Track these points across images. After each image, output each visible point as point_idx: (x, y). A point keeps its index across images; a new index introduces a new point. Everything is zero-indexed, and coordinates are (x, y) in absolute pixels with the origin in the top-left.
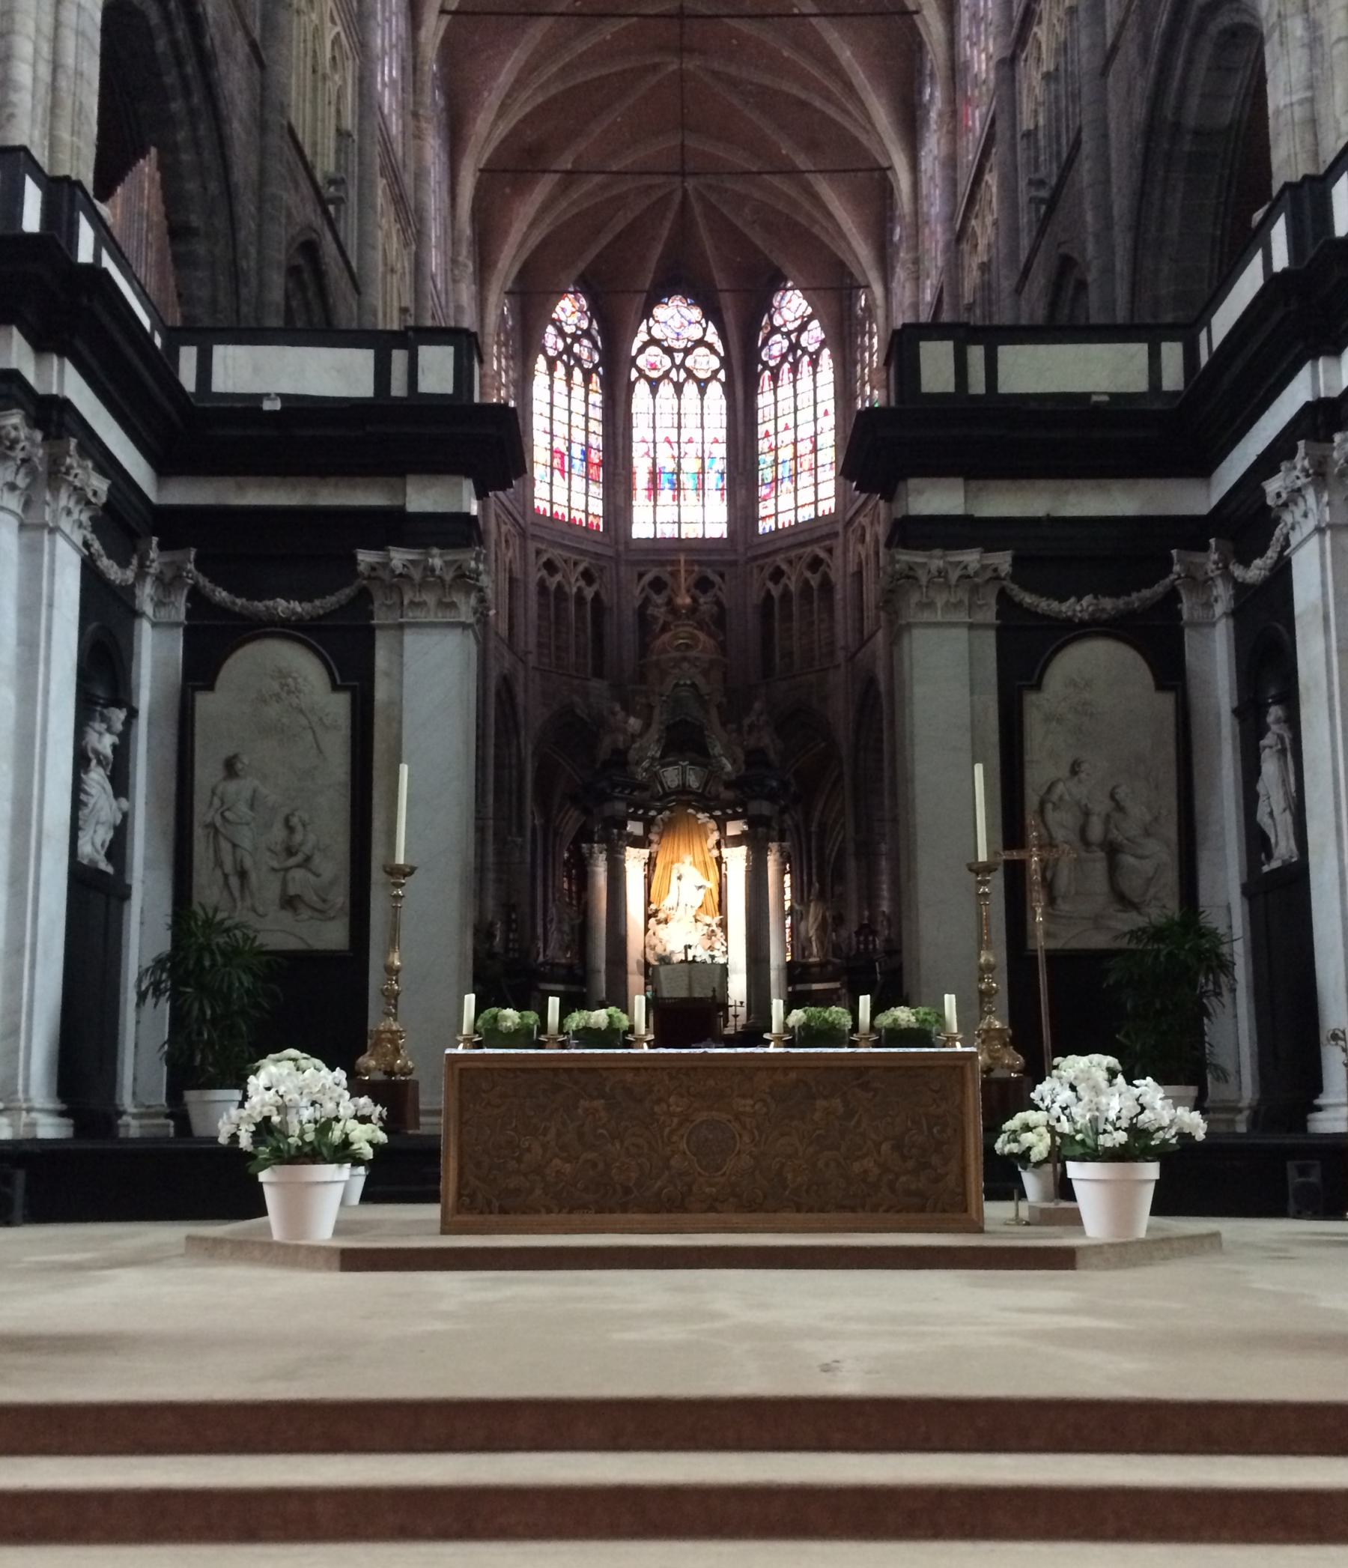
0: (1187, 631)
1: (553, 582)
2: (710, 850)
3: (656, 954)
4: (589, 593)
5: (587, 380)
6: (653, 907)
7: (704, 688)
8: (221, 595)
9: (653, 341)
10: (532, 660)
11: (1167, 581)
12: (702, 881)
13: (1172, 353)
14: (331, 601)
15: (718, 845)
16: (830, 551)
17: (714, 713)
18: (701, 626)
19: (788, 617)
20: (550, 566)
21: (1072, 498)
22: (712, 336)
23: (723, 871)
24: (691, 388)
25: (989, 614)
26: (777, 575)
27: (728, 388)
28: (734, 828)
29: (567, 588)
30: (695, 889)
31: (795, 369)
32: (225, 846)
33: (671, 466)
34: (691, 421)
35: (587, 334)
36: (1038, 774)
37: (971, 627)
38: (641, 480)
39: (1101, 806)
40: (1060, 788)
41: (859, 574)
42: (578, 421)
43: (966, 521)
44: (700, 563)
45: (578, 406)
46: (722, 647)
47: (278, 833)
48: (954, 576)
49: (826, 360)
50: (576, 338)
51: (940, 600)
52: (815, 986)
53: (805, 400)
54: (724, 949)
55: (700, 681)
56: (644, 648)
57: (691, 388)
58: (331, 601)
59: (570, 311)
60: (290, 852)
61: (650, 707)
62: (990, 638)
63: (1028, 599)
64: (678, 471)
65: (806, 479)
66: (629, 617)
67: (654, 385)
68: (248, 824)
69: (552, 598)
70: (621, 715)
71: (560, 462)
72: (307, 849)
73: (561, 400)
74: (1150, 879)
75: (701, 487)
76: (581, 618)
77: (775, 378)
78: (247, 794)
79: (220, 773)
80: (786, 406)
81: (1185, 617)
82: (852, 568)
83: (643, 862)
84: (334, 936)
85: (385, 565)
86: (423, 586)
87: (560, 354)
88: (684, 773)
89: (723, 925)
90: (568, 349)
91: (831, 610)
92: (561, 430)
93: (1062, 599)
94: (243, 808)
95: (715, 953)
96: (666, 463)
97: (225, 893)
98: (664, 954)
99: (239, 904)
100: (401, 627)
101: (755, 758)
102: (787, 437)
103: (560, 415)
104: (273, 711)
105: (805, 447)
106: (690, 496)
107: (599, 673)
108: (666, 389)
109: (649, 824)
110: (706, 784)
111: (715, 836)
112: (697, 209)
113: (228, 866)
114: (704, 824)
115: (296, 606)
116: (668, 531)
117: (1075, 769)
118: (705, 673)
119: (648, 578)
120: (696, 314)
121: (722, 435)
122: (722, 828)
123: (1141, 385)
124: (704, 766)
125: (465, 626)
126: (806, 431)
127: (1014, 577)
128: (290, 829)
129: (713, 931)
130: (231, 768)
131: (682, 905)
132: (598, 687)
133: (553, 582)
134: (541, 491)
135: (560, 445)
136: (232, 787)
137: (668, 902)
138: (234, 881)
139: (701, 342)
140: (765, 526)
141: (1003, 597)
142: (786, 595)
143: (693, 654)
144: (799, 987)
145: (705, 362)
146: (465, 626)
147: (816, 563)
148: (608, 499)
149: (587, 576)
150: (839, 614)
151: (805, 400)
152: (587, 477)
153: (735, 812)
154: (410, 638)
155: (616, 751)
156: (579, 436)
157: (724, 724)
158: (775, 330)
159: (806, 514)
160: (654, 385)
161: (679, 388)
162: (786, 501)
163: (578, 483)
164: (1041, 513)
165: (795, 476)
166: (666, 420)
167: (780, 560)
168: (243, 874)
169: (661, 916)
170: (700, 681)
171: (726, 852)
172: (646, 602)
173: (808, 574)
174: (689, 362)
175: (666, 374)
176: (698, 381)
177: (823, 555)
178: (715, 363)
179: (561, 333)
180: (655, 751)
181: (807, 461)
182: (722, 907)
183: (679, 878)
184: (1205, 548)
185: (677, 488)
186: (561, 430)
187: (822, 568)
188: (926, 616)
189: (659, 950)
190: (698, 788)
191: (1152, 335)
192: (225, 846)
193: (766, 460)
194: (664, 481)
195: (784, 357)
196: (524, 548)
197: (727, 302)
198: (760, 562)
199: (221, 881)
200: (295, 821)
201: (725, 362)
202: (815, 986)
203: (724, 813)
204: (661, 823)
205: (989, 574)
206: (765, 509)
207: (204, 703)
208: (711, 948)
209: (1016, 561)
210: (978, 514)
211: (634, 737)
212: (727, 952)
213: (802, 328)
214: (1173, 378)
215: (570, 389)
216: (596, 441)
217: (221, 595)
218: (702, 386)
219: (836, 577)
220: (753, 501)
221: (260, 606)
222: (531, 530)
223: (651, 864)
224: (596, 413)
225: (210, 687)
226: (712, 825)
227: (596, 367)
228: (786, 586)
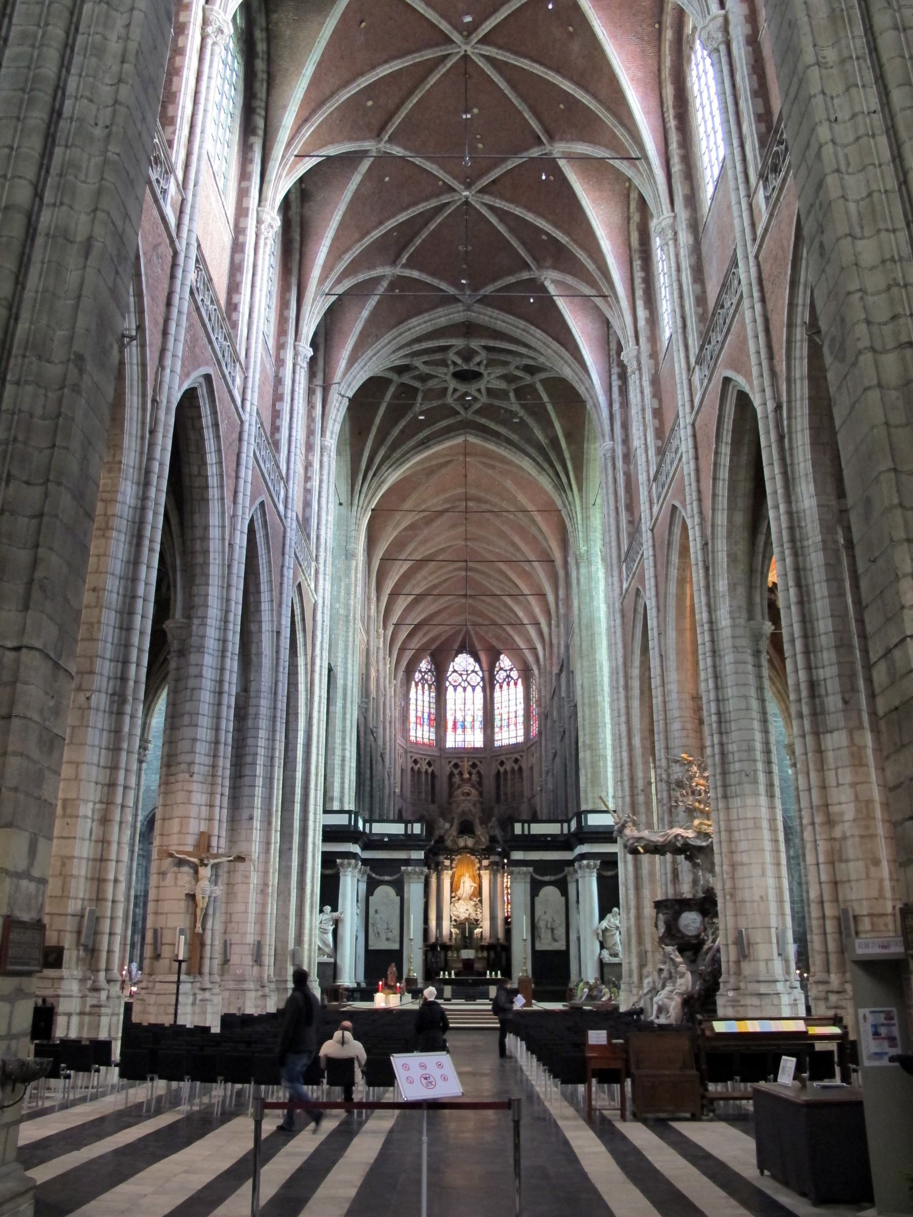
1: (416, 768)
4: (430, 770)
5: (430, 686)
9: (455, 671)
10: (409, 800)
13: (565, 825)
14: (395, 877)
15: (479, 869)
17: (477, 822)
18: (473, 786)
19: (506, 779)
20: (415, 762)
22: (477, 668)
24: (469, 689)
25: (528, 880)
26: (502, 763)
27: (484, 689)
28: (485, 863)
31: (508, 684)
33: (461, 719)
34: (469, 702)
35: (430, 671)
36: (538, 913)
38: (450, 724)
39: (550, 920)
41: (532, 768)
42: (426, 704)
45: (426, 698)
46: (481, 794)
47: (385, 926)
49: (520, 681)
50: (426, 673)
53: (512, 697)
55: (472, 808)
56: (451, 795)
58: (395, 877)
59: (424, 665)
61: (453, 818)
64: (464, 721)
65: (512, 727)
66: (445, 779)
67: (455, 687)
69: (416, 774)
71: (419, 721)
73: (420, 697)
75: (473, 727)
76: (426, 779)
77: (501, 687)
80: (505, 698)
84: (396, 946)
89: (481, 901)
90: (423, 678)
92: (420, 708)
96: (460, 718)
101: (493, 840)
102: (505, 710)
103: (420, 703)
105: (512, 715)
106: (469, 731)
107: (433, 802)
108: (460, 689)
109: (452, 861)
112: (472, 633)
116: (460, 745)
118: (474, 805)
120: (471, 660)
121: (481, 706)
122: (480, 862)
126: (513, 709)
127: (535, 871)
130: (376, 912)
132: (433, 808)
133: (416, 768)
134: (412, 733)
135: (419, 714)
139: (473, 671)
140: (497, 744)
141: (532, 877)
142: (506, 771)
145: (476, 679)
147: (516, 761)
148: (437, 733)
149: (429, 764)
151: (512, 697)
152: (429, 725)
156: (426, 710)
158: (501, 669)
159: (513, 741)
160: (455, 687)
161: (465, 689)
162: (505, 735)
163: (426, 728)
165: (508, 725)
166: (460, 701)
167: (503, 758)
170: (472, 808)
172: (451, 775)
178: (479, 679)
179: (420, 672)
180: (455, 833)
181: (513, 721)
182: (480, 893)
185: (464, 727)
186: (420, 708)
191: (561, 822)
193: (497, 718)
194: (459, 725)
197: (483, 656)
201: (483, 679)
206: (497, 736)
211: (447, 830)
213: (511, 670)
214: (566, 831)
216: (433, 711)
218: (474, 688)
219: (524, 767)
220: (493, 733)
223: (452, 877)
224: (433, 700)
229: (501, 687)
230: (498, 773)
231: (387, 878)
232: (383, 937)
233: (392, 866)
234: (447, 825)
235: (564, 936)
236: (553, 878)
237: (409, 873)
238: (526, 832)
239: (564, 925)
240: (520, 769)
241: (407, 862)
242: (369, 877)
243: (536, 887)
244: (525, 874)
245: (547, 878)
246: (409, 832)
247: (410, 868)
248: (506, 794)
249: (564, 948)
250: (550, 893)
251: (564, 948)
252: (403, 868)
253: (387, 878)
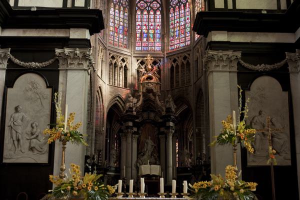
0: (291, 75)
1: (114, 62)
4: (124, 65)
5: (124, 8)
6: (140, 151)
7: (155, 91)
8: (17, 61)
11: (285, 61)
14: (47, 63)
16: (189, 55)
17: (157, 98)
19: (177, 72)
21: (257, 37)
25: (235, 69)
31: (179, 8)
32: (14, 132)
37: (230, 72)
40: (256, 118)
43: (228, 42)
44: (154, 57)
45: (122, 16)
46: (160, 79)
47: (29, 129)
48: (225, 58)
51: (221, 64)
57: (152, 13)
58: (47, 63)
60: (32, 134)
62: (236, 75)
63: (246, 65)
64: (148, 33)
68: (20, 126)
70: (132, 98)
72: (37, 134)
74: (282, 145)
75: (154, 38)
77: (174, 10)
78: (21, 117)
79: (14, 111)
81: (290, 70)
82: (195, 59)
84: (44, 159)
85: (63, 53)
86: (74, 59)
87: (117, 3)
89: (159, 157)
91: (189, 70)
93: (256, 65)
94: (19, 121)
97: (13, 146)
99: (17, 149)
100: (67, 70)
104: (30, 93)
108: (145, 13)
113: (15, 138)
115: (38, 64)
117: (260, 113)
119: (139, 61)
121: (160, 24)
123: (276, 8)
125: (85, 70)
128: (33, 127)
130: (16, 110)
136: (17, 115)
138: (16, 142)
141: (239, 64)
143: (152, 81)
146: (85, 70)
150: (191, 72)
152: (123, 34)
154: (69, 73)
155: (130, 108)
161: (149, 12)
164: (249, 41)
168: (18, 140)
173: (183, 61)
174: (151, 5)
175: (146, 8)
176: (154, 10)
177: (187, 56)
178: (159, 6)
184: (295, 52)
185: (148, 37)
187: (187, 59)
188: (218, 69)
192: (14, 132)
195: (177, 4)
196: (106, 53)
198: (170, 57)
199: (12, 142)
200: (34, 125)
201: (161, 5)
205: (235, 57)
207: (9, 90)
209: (242, 54)
210: (231, 41)
215: (120, 12)
217: (17, 61)
221: (27, 64)
222: (108, 48)
225: (12, 87)
227: (127, 6)
228: (177, 64)
229: (174, 10)
230: (172, 67)
231: (34, 64)
232: (25, 145)
233: (44, 47)
234: (135, 100)
235: (288, 145)
236: (269, 67)
237: (65, 58)
238: (230, 7)
239: (288, 131)
240: (188, 64)
241: (65, 42)
242: (10, 61)
243: (245, 79)
244: (229, 60)
245: (260, 67)
246: (69, 5)
247: (67, 51)
248: (177, 82)
249: (289, 163)
250: (265, 85)
251: (289, 163)
252: (58, 51)
253: (34, 64)
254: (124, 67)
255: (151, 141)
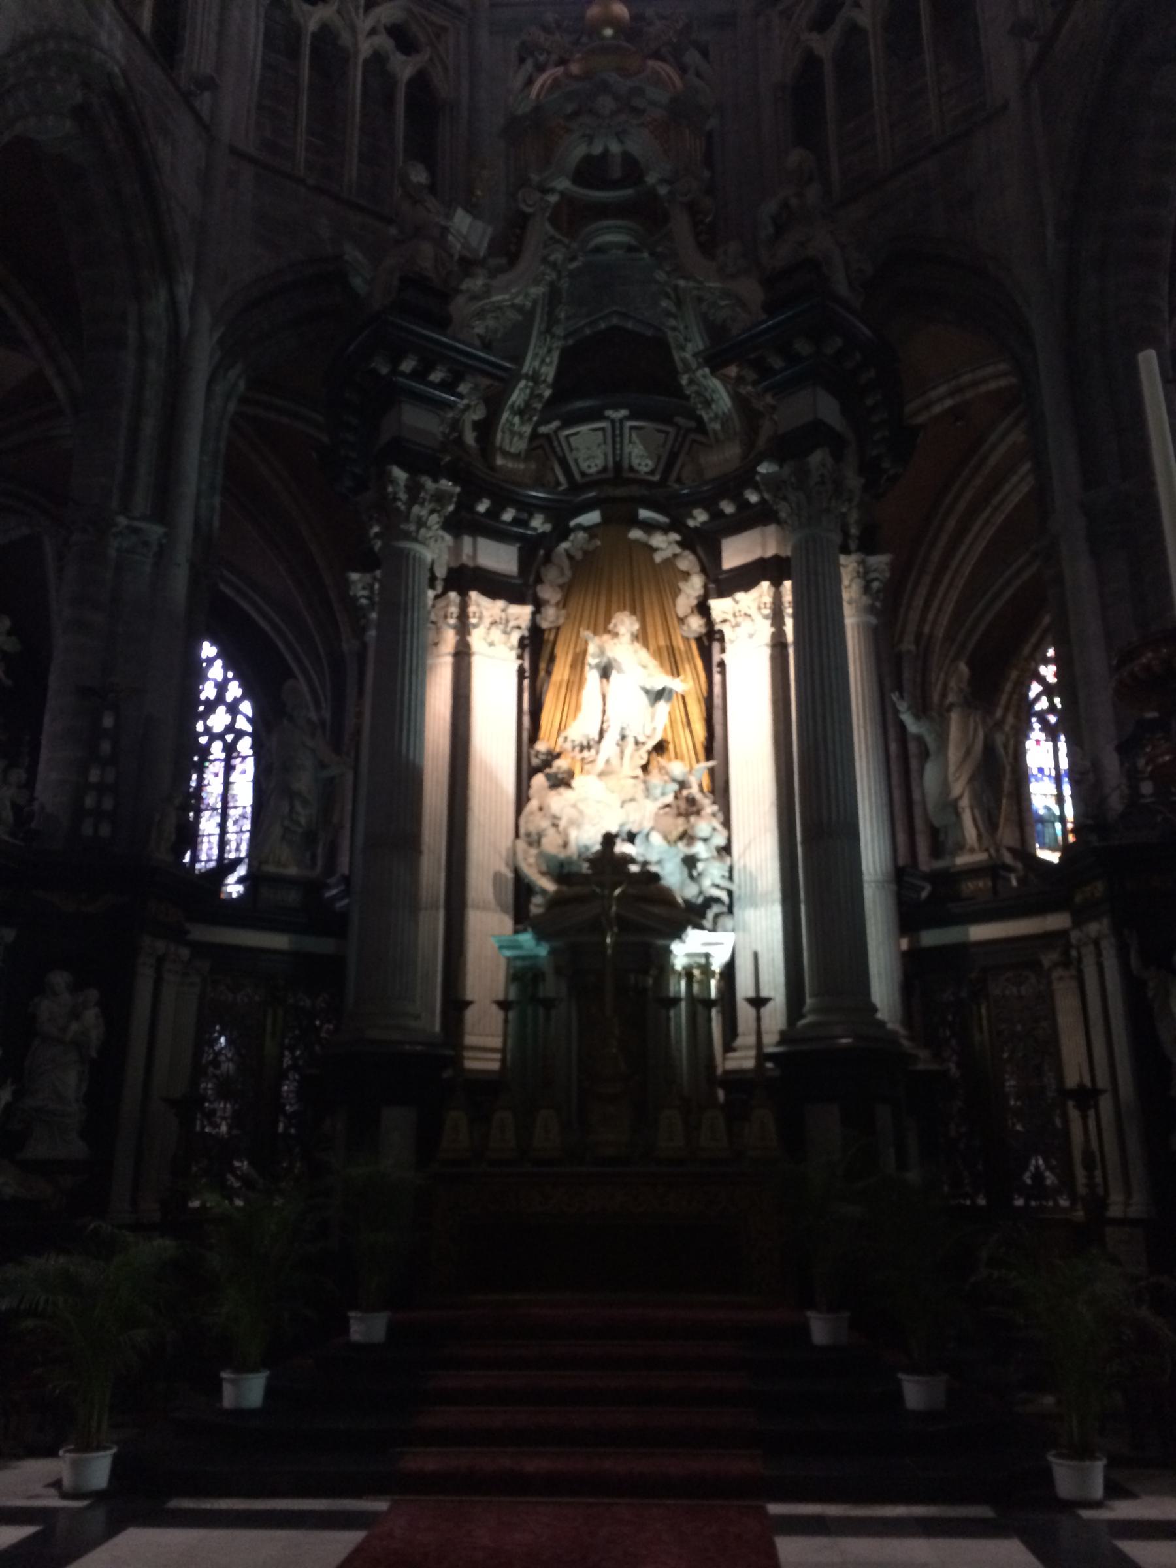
2: (682, 621)
3: (542, 855)
4: (404, 68)
6: (541, 746)
12: (660, 679)
23: (716, 657)
29: (346, 39)
30: (644, 700)
52: (979, 932)
54: (720, 840)
83: (515, 637)
88: (616, 436)
89: (720, 789)
95: (700, 849)
98: (562, 855)
110: (669, 466)
111: (695, 586)
114: (670, 562)
124: (663, 417)
129: (691, 801)
131: (611, 737)
137: (582, 728)
144: (930, 938)
153: (743, 505)
157: (707, 248)
169: (561, 764)
171: (719, 607)
183: (605, 672)
189: (550, 845)
190: (652, 472)
202: (979, 932)
203: (716, 514)
204: (566, 563)
208: (687, 837)
211: (468, 265)
212: (726, 850)
226: (687, 562)
230: (811, 61)
254: (411, 83)
255: (644, 655)
